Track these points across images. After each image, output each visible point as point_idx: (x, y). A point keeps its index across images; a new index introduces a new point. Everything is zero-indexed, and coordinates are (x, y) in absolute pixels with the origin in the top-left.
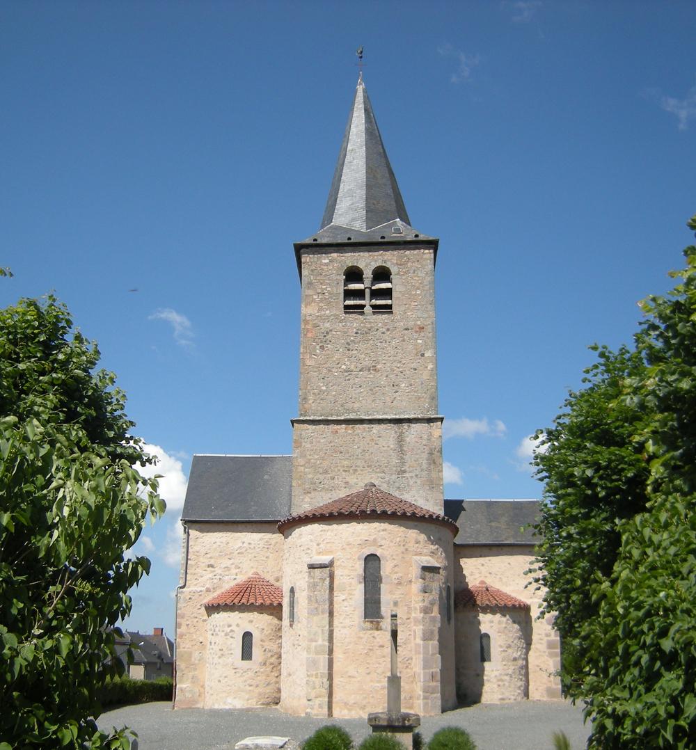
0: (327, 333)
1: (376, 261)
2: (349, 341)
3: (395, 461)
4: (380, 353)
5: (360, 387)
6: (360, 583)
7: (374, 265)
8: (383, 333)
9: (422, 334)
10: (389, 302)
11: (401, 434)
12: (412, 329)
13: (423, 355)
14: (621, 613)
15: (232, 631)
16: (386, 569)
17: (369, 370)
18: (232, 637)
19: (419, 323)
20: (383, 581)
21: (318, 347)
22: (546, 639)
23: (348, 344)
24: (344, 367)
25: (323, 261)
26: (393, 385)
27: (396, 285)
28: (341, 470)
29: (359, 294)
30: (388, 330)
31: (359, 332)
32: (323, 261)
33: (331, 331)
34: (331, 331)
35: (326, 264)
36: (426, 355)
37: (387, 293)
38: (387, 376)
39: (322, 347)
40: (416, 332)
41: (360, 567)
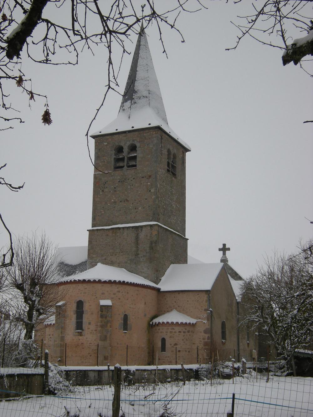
0: (105, 183)
1: (129, 141)
2: (115, 186)
3: (134, 249)
4: (130, 192)
5: (120, 210)
6: (74, 314)
7: (128, 143)
8: (132, 181)
9: (150, 179)
10: (134, 163)
11: (138, 234)
12: (145, 177)
13: (150, 191)
14: (46, 350)
15: (50, 338)
16: (86, 307)
17: (124, 201)
18: (50, 341)
19: (149, 173)
20: (84, 312)
21: (101, 191)
22: (203, 341)
23: (115, 188)
24: (113, 200)
25: (105, 144)
26: (135, 209)
27: (139, 154)
28: (110, 254)
29: (122, 160)
30: (134, 179)
31: (120, 181)
32: (105, 144)
33: (107, 181)
34: (107, 181)
35: (106, 145)
36: (152, 191)
37: (135, 158)
38: (133, 204)
39: (103, 191)
40: (147, 178)
41: (74, 306)
